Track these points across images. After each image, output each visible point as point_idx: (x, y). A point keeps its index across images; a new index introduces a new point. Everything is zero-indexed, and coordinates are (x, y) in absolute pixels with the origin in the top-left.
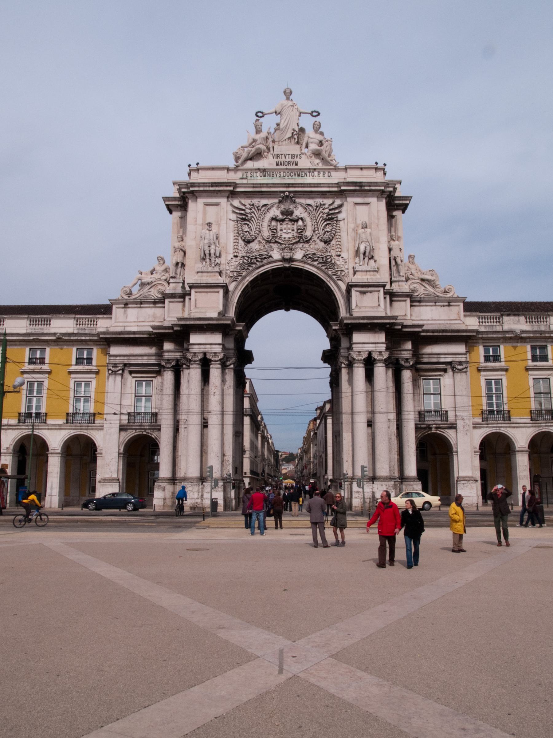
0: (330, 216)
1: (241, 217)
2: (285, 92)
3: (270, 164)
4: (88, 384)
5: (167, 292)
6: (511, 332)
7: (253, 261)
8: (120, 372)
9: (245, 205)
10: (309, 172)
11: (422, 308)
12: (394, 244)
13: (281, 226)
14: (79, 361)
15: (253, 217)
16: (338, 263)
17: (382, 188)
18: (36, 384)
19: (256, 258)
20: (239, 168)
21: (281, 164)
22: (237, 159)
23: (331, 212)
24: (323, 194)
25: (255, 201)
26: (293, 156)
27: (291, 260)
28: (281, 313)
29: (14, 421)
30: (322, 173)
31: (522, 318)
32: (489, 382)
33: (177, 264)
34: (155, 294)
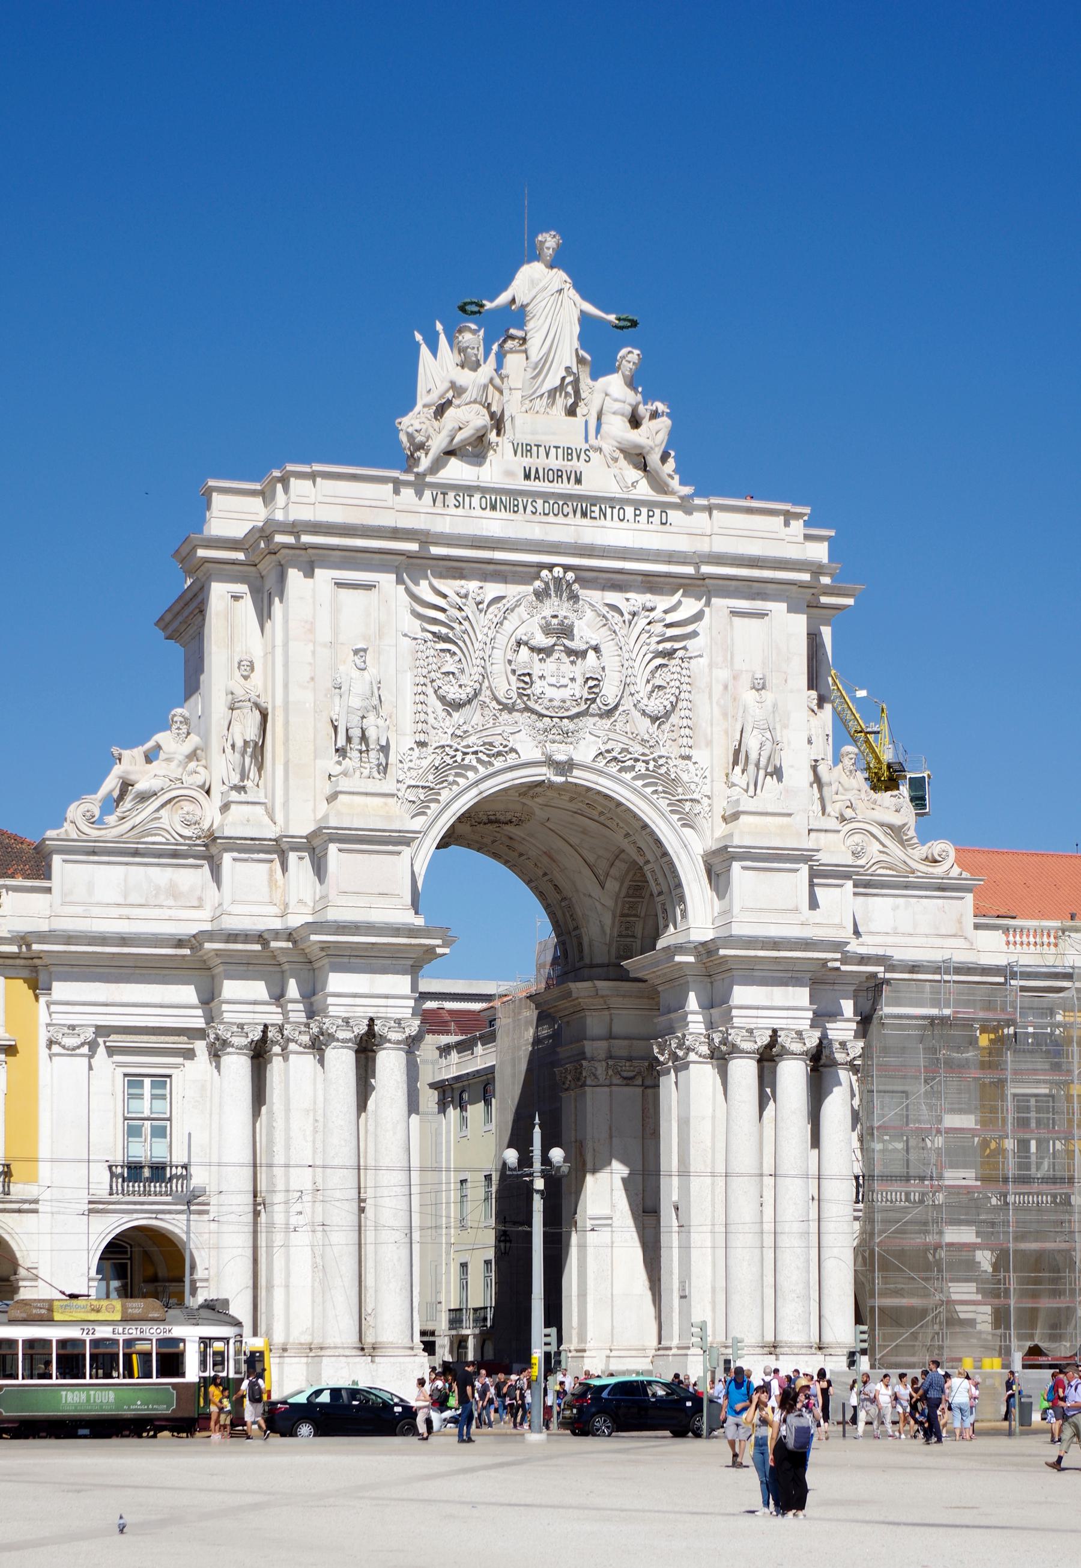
0: (668, 645)
1: (435, 628)
3: (509, 473)
7: (466, 762)
8: (85, 1050)
9: (445, 596)
10: (612, 508)
11: (871, 899)
13: (543, 665)
15: (465, 632)
16: (685, 777)
19: (476, 753)
20: (428, 479)
21: (537, 478)
23: (670, 632)
26: (568, 453)
30: (644, 511)
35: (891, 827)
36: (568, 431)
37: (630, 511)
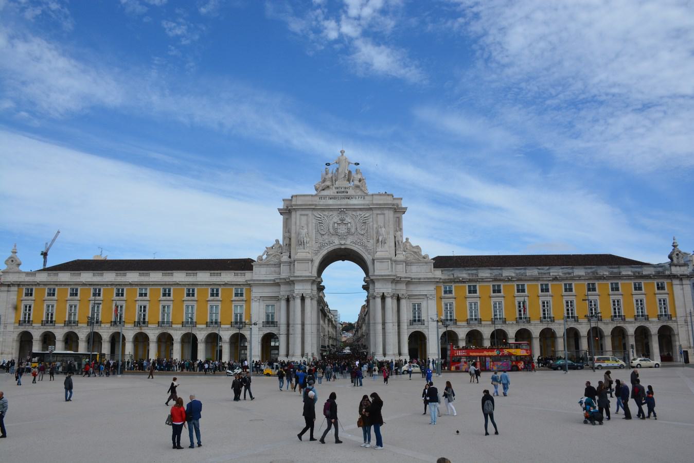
2: (341, 152)
3: (334, 193)
4: (241, 306)
5: (282, 260)
6: (458, 278)
8: (258, 301)
12: (398, 233)
14: (236, 295)
16: (368, 245)
17: (391, 206)
18: (214, 307)
22: (317, 190)
24: (360, 209)
25: (326, 213)
26: (345, 188)
27: (345, 244)
28: (341, 261)
29: (204, 326)
31: (465, 272)
32: (446, 305)
33: (286, 245)
34: (275, 260)
35: (415, 252)
36: (346, 184)
37: (357, 197)
